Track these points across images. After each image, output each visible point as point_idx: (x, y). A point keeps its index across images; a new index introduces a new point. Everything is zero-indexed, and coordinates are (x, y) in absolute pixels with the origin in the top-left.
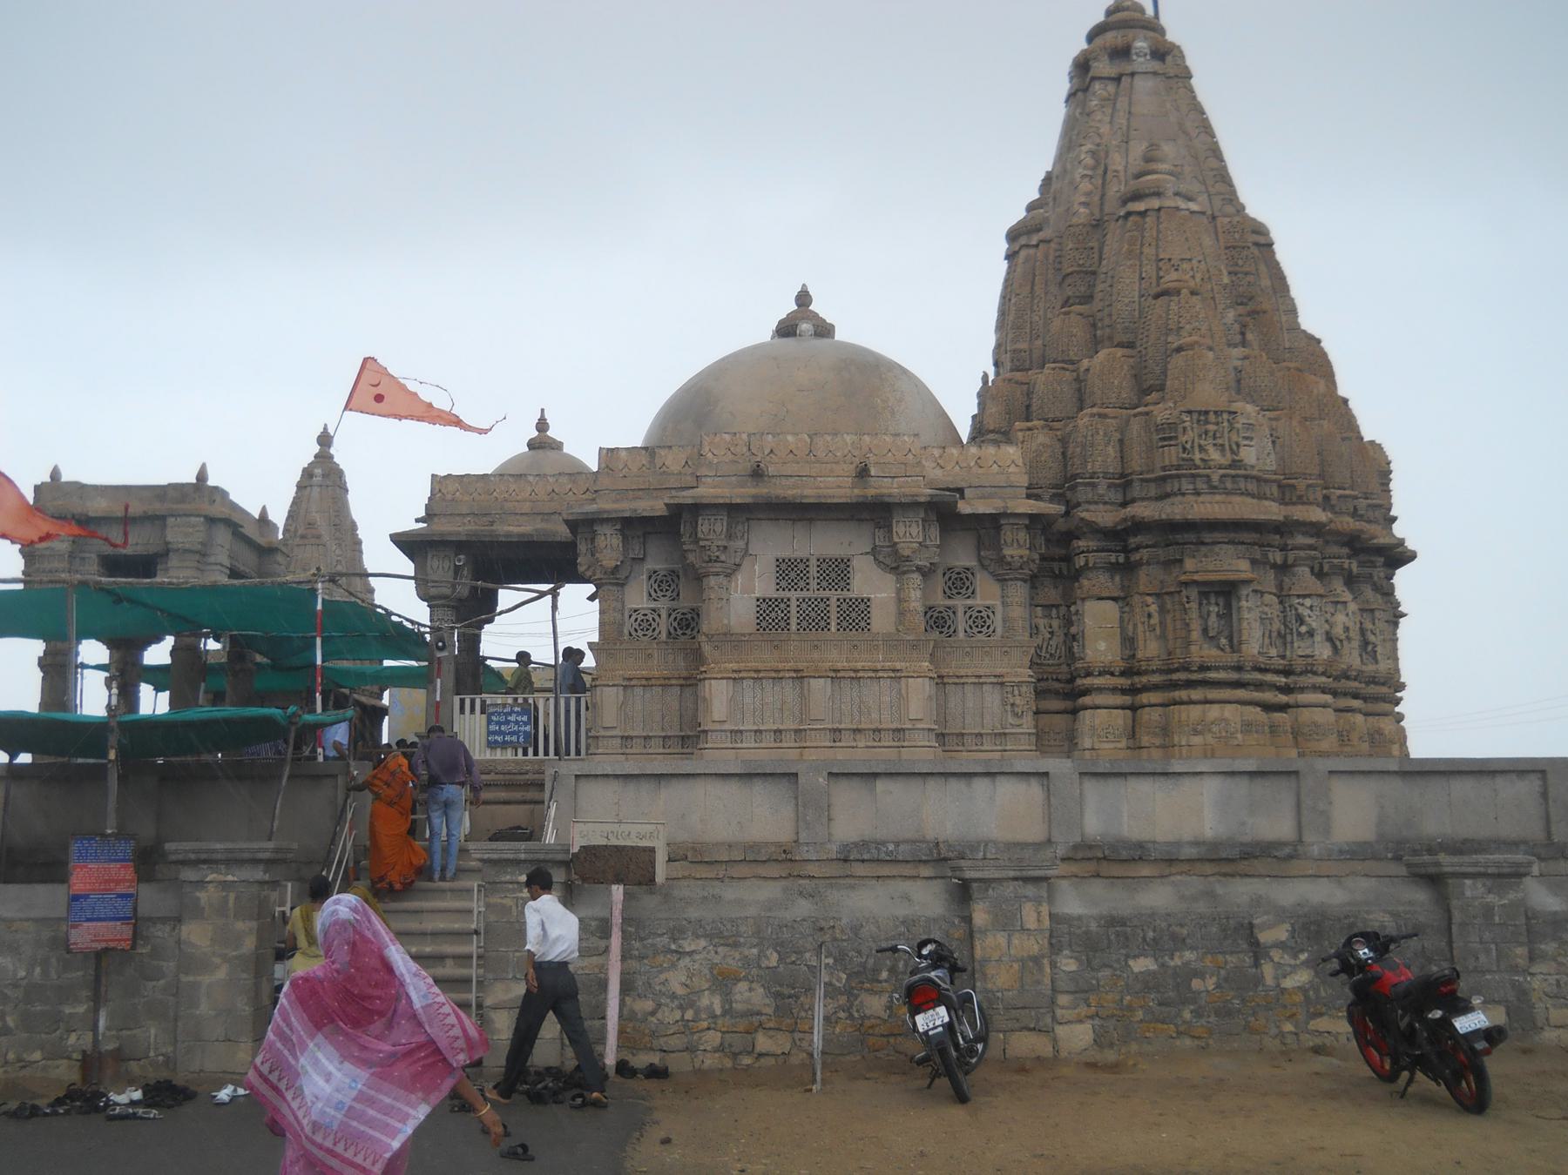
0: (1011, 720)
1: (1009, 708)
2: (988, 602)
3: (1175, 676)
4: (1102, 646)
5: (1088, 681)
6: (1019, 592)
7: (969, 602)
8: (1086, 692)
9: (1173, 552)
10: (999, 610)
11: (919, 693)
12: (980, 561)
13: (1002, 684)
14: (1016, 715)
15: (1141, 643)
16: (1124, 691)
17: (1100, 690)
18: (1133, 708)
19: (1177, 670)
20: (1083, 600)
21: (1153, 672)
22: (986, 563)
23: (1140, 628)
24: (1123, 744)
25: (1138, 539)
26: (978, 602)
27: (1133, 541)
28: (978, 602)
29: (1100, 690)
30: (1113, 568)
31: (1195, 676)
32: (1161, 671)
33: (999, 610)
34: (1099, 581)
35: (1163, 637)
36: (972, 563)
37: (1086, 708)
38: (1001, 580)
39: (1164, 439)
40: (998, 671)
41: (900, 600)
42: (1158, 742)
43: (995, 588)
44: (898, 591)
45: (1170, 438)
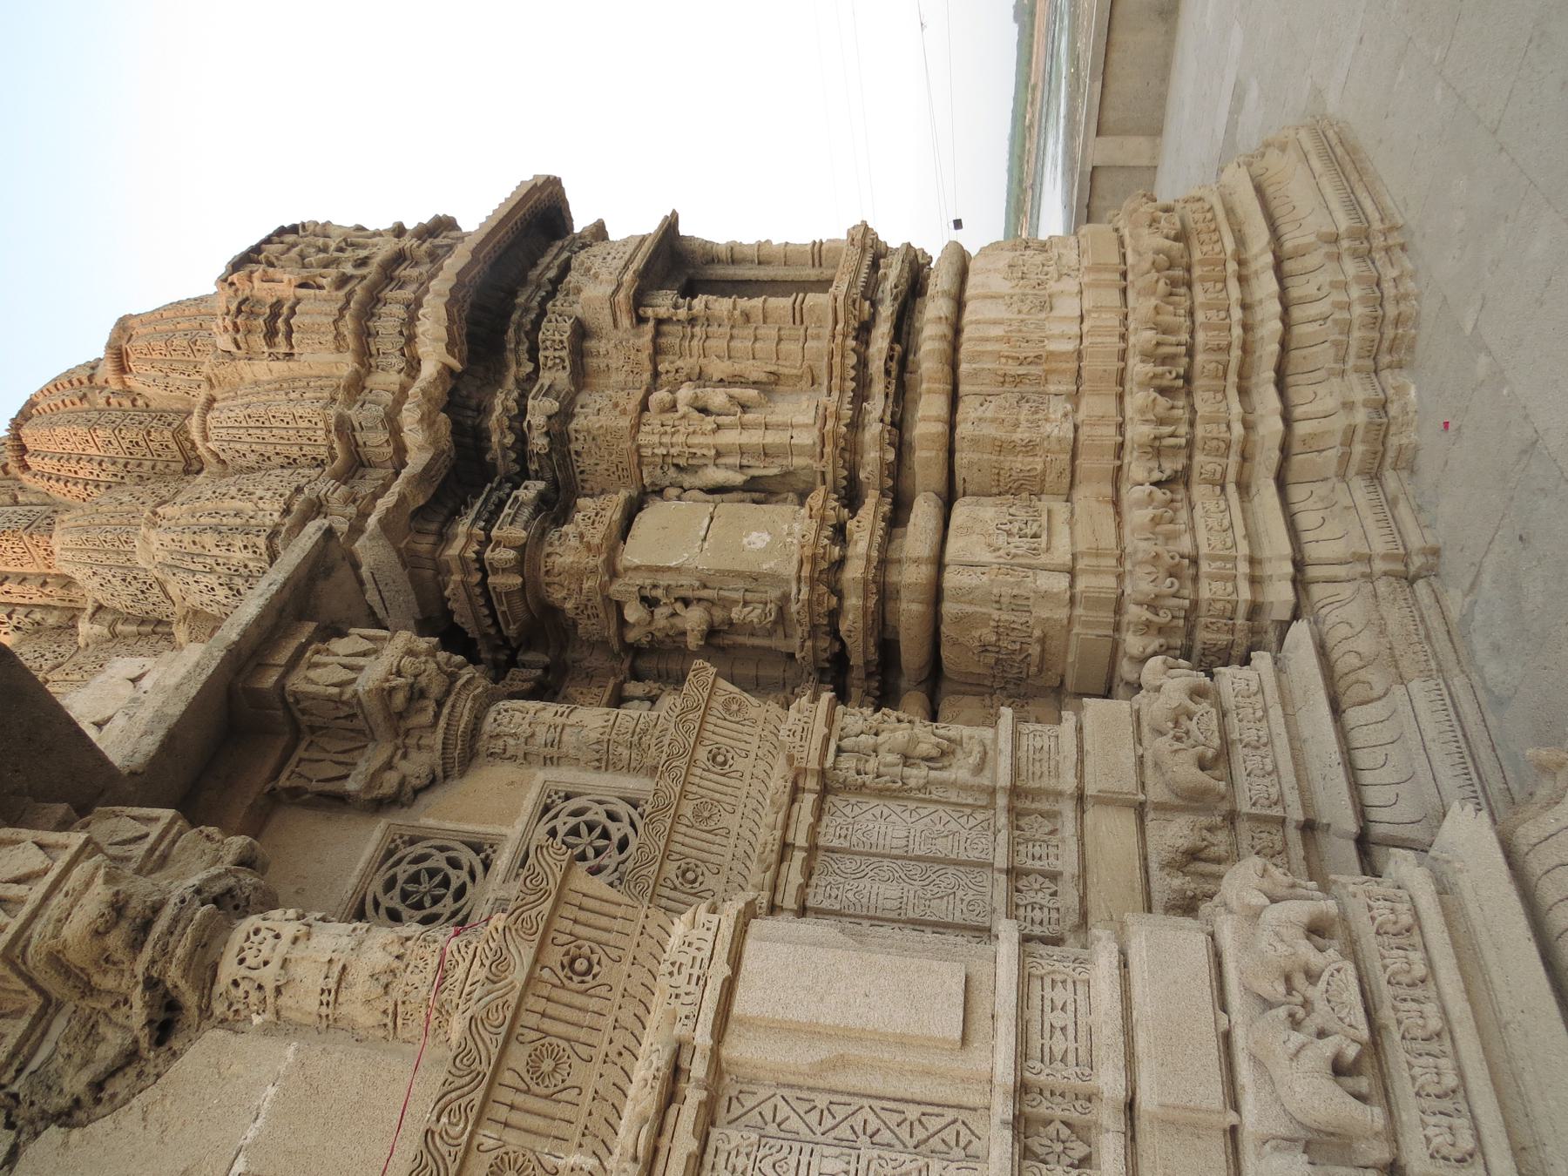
0: (960, 771)
1: (917, 775)
2: (530, 800)
3: (877, 366)
4: (758, 539)
5: (854, 571)
6: (521, 717)
7: (502, 862)
8: (888, 649)
9: (556, 332)
10: (566, 776)
11: (817, 994)
12: (380, 805)
13: (825, 791)
14: (942, 756)
15: (771, 438)
16: (897, 518)
17: (884, 562)
18: (948, 499)
19: (863, 363)
20: (614, 574)
21: (856, 425)
22: (391, 781)
23: (729, 438)
24: (1060, 509)
25: (496, 418)
26: (512, 833)
27: (499, 438)
28: (512, 833)
29: (884, 562)
30: (556, 508)
31: (887, 310)
32: (861, 394)
33: (566, 776)
34: (571, 550)
35: (770, 385)
36: (372, 836)
37: (937, 594)
38: (466, 753)
39: (271, 335)
40: (778, 780)
41: (330, 1023)
42: (1058, 408)
43: (489, 779)
44: (280, 1026)
45: (275, 315)
